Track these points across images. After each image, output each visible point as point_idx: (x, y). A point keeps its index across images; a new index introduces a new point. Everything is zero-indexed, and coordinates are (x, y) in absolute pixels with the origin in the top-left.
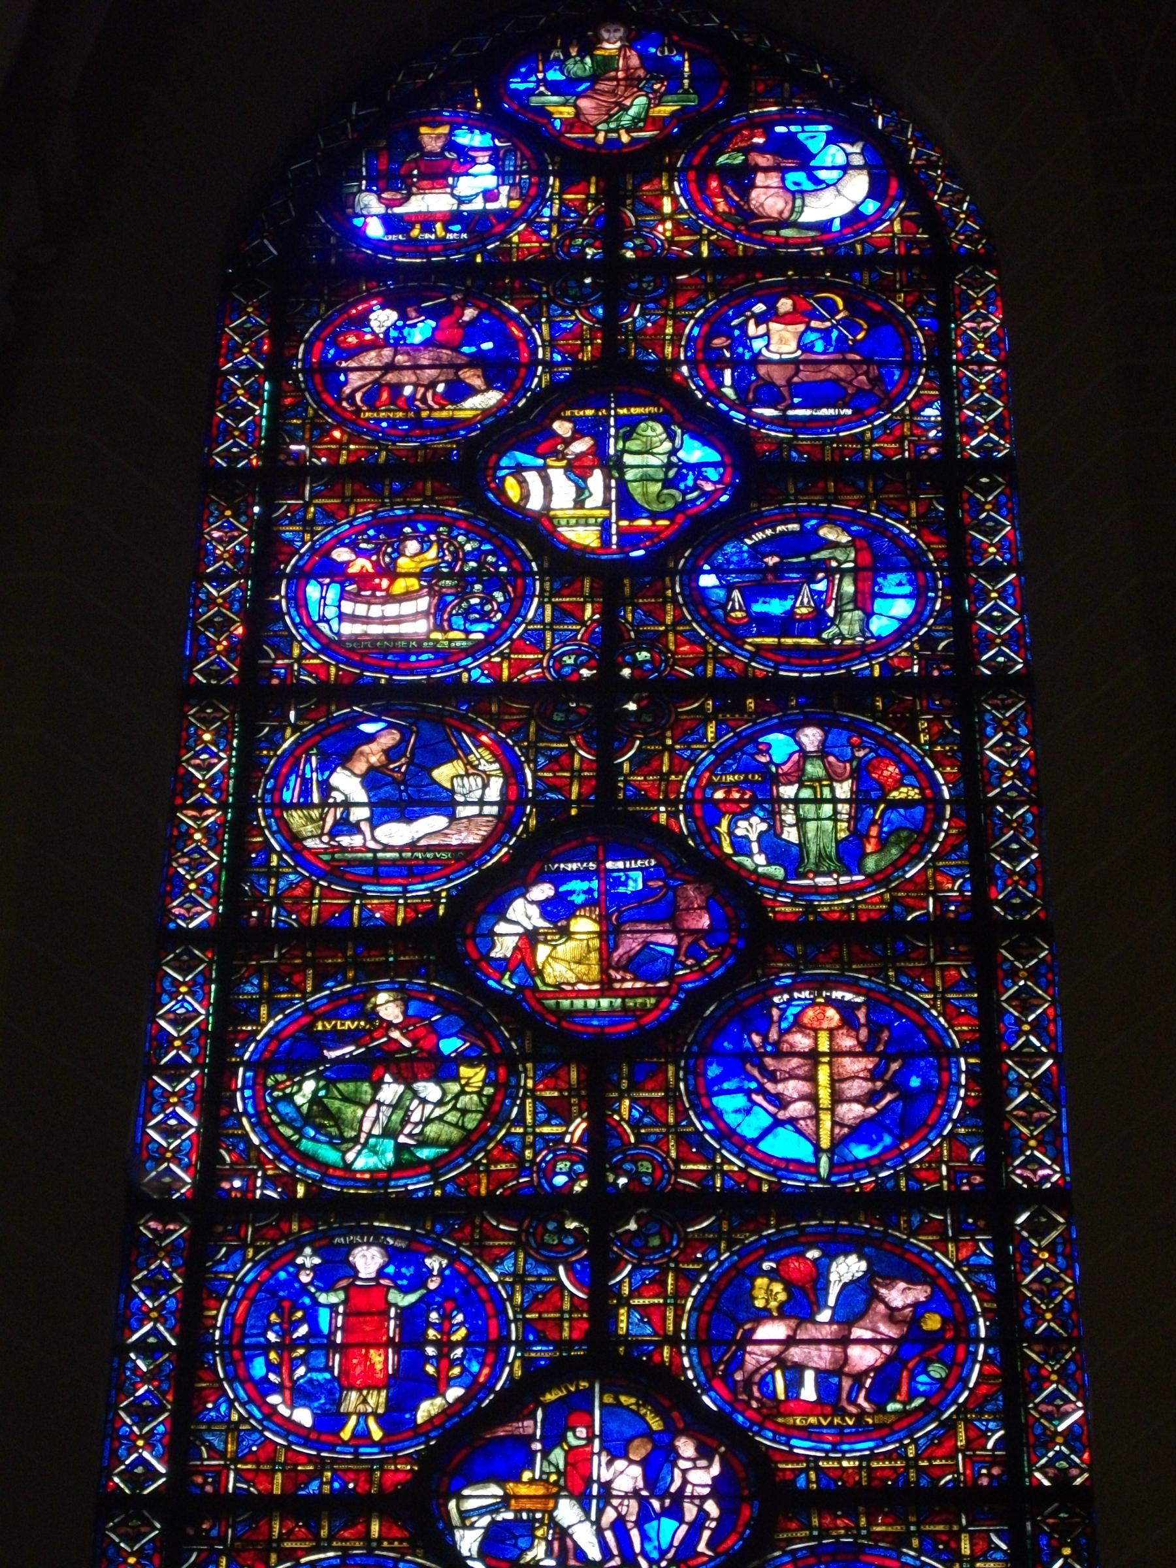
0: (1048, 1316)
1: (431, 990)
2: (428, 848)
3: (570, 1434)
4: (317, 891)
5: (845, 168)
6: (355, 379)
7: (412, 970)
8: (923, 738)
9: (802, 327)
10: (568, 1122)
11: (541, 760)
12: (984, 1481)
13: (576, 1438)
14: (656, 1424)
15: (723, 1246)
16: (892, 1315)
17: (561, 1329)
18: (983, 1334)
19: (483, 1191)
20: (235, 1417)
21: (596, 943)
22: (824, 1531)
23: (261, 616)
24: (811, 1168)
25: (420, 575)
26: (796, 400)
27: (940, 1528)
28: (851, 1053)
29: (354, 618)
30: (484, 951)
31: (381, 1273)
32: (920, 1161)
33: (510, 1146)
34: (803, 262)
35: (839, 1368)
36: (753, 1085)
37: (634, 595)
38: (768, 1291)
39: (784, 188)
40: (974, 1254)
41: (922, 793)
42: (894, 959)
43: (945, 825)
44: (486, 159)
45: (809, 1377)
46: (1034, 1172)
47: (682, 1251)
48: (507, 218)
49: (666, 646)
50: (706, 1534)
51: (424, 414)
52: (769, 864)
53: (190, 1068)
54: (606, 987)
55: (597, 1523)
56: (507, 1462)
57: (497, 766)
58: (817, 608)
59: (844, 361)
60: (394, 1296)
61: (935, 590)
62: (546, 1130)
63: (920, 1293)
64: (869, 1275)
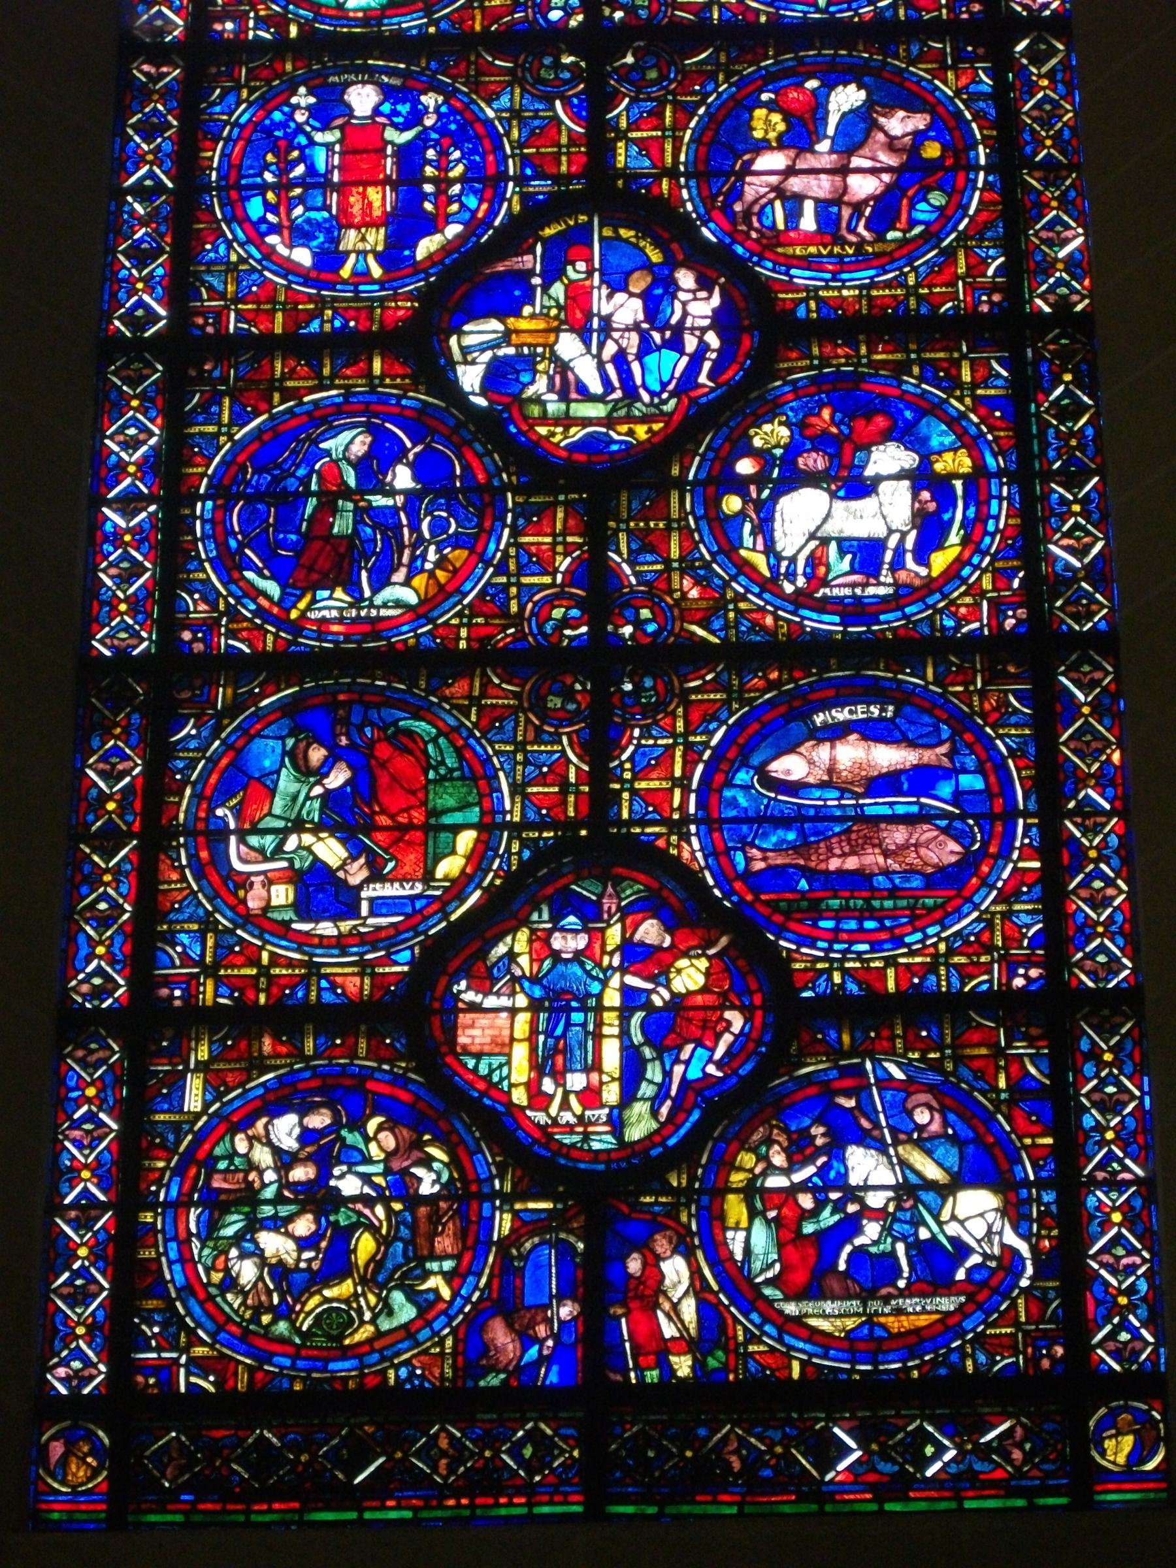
0: (1048, 142)
3: (569, 268)
12: (985, 308)
13: (575, 272)
14: (655, 257)
15: (721, 77)
16: (892, 144)
17: (559, 164)
18: (982, 161)
19: (478, 27)
22: (825, 361)
27: (941, 355)
31: (376, 111)
38: (767, 121)
40: (973, 82)
45: (809, 207)
47: (680, 83)
50: (707, 365)
55: (598, 356)
56: (506, 298)
60: (390, 134)
63: (920, 122)
64: (869, 104)
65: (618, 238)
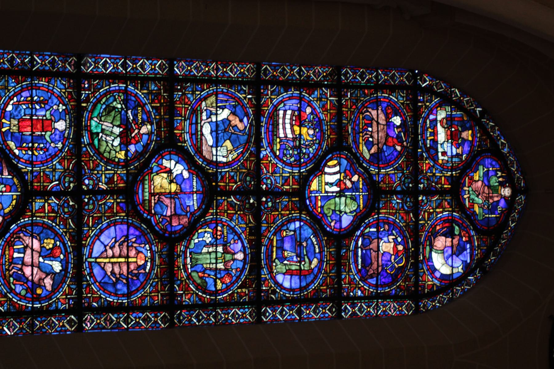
0: (41, 325)
1: (152, 142)
2: (201, 139)
3: (3, 186)
4: (186, 106)
5: (452, 267)
6: (374, 113)
7: (158, 135)
8: (239, 290)
9: (392, 253)
10: (106, 184)
11: (232, 174)
14: (7, 211)
15: (65, 230)
17: (37, 183)
18: (35, 306)
19: (83, 159)
20: (9, 88)
21: (168, 191)
23: (287, 85)
24: (90, 256)
25: (300, 134)
26: (364, 251)
28: (128, 268)
29: (285, 115)
30: (165, 157)
31: (56, 129)
32: (92, 288)
33: (98, 167)
34: (416, 254)
35: (23, 264)
36: (118, 239)
37: (292, 201)
38: (49, 243)
39: (445, 247)
40: (62, 303)
41: (219, 290)
42: (161, 281)
43: (208, 297)
44: (458, 152)
45: (22, 255)
46: (89, 322)
48: (435, 158)
49: (274, 211)
51: (361, 134)
52: (195, 244)
53: (126, 70)
54: (154, 194)
57: (231, 160)
58: (286, 258)
59: (378, 266)
61: (293, 294)
62: (103, 177)
63: (49, 288)
64: (55, 273)
65: (13, 200)
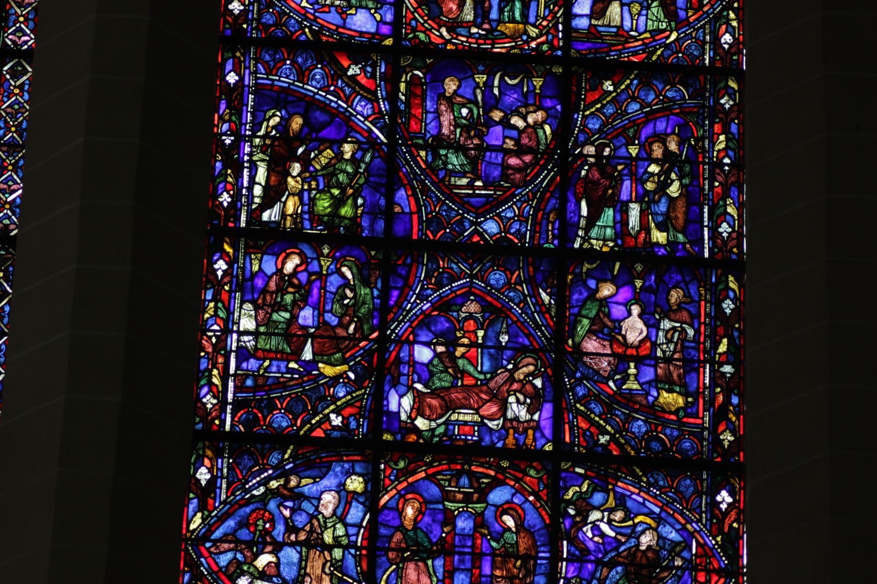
46: (19, 38)
